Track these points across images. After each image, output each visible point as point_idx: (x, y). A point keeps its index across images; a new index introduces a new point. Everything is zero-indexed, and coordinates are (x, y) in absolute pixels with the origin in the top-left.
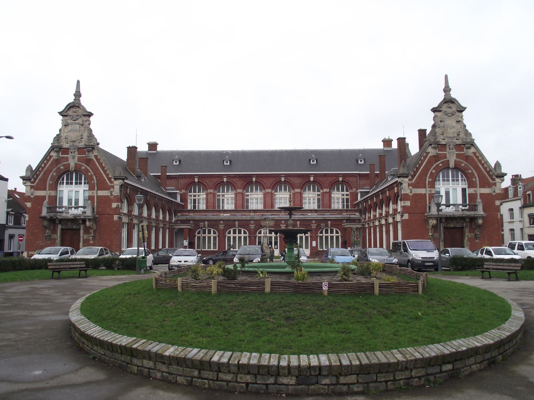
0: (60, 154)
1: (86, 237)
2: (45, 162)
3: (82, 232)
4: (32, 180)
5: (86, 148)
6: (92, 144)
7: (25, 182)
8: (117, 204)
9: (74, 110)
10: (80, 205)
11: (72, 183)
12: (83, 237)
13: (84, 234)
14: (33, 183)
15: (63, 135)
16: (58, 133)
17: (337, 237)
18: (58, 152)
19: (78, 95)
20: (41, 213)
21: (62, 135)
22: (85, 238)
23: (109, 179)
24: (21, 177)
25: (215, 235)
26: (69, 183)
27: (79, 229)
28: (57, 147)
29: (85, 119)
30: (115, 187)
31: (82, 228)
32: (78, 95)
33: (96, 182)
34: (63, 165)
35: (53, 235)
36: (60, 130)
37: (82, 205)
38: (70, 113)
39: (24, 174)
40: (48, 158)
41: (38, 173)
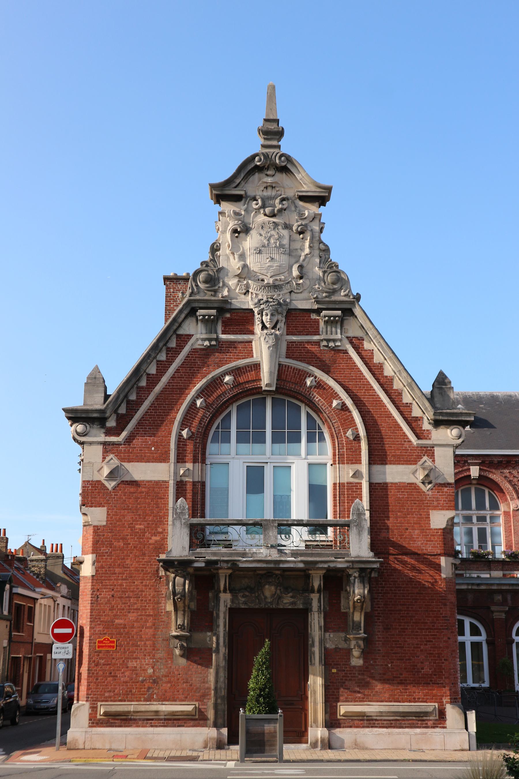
0: (220, 328)
1: (334, 639)
2: (162, 357)
3: (316, 621)
4: (111, 423)
5: (318, 311)
6: (341, 296)
7: (80, 428)
8: (450, 514)
9: (269, 180)
10: (294, 516)
11: (260, 439)
12: (322, 641)
13: (326, 628)
14: (109, 432)
15: (231, 263)
16: (207, 257)
17: (476, 646)
18: (209, 323)
19: (272, 132)
20: (161, 547)
21: (222, 263)
22: (330, 645)
23: (413, 423)
24: (64, 410)
25: (476, 639)
26: (252, 435)
27: (306, 612)
28: (202, 307)
29: (310, 209)
30: (437, 451)
31: (315, 604)
32: (272, 132)
33: (362, 432)
34: (237, 372)
35: (198, 636)
36: (215, 249)
37: (304, 516)
38: (255, 186)
39: (78, 402)
40: (173, 344)
41: (133, 397)
